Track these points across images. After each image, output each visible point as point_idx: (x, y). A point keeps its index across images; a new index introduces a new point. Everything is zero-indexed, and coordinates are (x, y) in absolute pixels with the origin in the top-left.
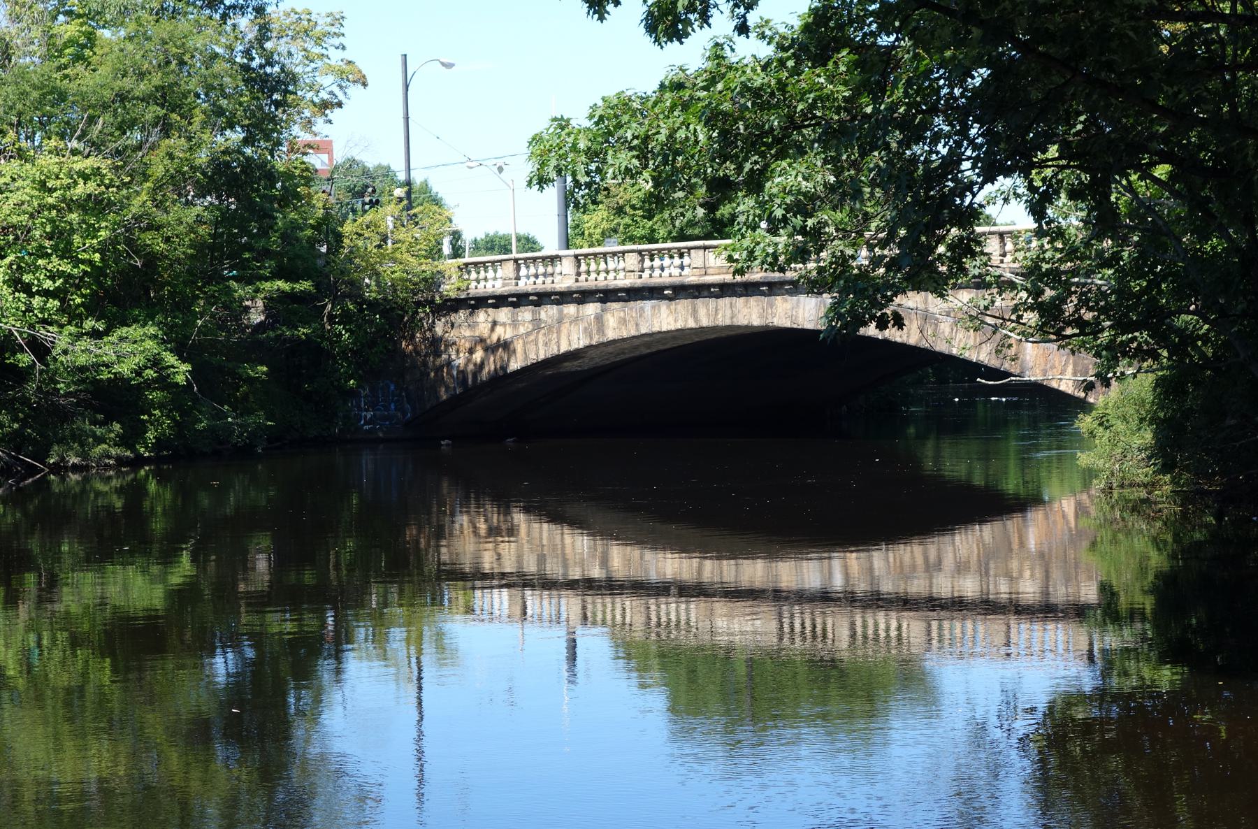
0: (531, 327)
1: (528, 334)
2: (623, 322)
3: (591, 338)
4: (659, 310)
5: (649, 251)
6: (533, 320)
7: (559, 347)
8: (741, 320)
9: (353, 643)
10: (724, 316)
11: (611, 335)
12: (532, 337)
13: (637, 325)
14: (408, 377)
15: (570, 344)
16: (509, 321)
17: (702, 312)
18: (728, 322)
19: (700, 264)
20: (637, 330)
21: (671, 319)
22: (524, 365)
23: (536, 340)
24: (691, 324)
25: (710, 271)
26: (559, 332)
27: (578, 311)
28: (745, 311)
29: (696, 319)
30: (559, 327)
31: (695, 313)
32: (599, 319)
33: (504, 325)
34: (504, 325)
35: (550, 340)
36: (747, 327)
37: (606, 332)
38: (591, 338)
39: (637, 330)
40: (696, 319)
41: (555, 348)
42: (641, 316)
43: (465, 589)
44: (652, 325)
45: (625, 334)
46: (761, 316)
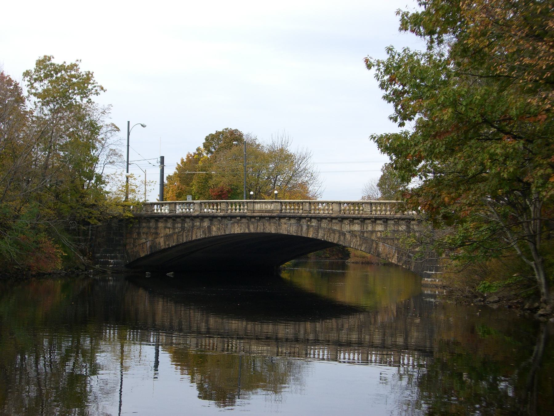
0: (180, 229)
1: (179, 232)
2: (219, 229)
3: (205, 235)
4: (234, 225)
5: (239, 202)
6: (182, 227)
7: (192, 238)
8: (267, 231)
9: (285, 384)
10: (260, 229)
11: (214, 234)
12: (181, 233)
13: (225, 230)
14: (128, 247)
15: (196, 237)
16: (171, 227)
17: (251, 227)
18: (262, 231)
19: (252, 208)
20: (225, 232)
21: (239, 229)
22: (177, 244)
23: (183, 235)
24: (247, 231)
25: (255, 211)
26: (192, 232)
27: (200, 224)
28: (269, 227)
29: (249, 229)
30: (193, 230)
31: (248, 228)
32: (209, 227)
33: (169, 228)
34: (169, 228)
35: (188, 235)
36: (269, 233)
37: (212, 232)
38: (205, 235)
39: (225, 232)
40: (249, 229)
41: (191, 238)
42: (226, 227)
43: (291, 347)
44: (231, 231)
45: (219, 234)
46: (275, 230)
